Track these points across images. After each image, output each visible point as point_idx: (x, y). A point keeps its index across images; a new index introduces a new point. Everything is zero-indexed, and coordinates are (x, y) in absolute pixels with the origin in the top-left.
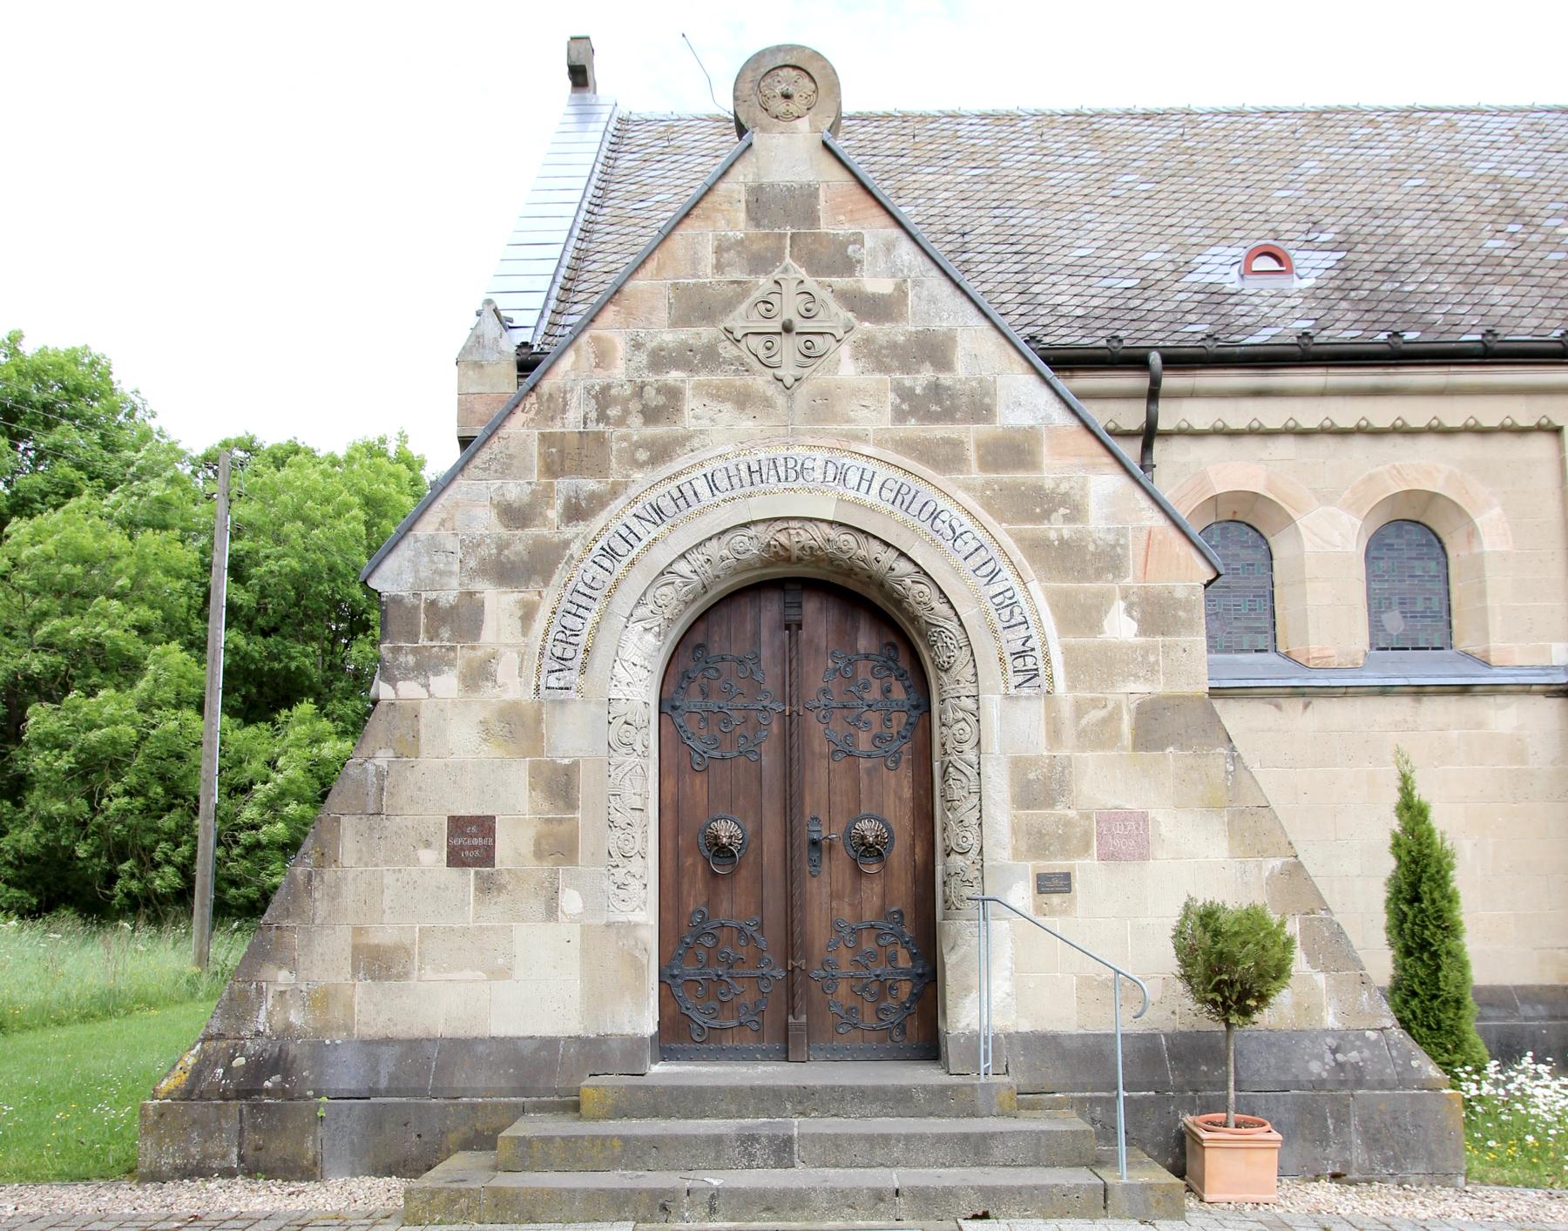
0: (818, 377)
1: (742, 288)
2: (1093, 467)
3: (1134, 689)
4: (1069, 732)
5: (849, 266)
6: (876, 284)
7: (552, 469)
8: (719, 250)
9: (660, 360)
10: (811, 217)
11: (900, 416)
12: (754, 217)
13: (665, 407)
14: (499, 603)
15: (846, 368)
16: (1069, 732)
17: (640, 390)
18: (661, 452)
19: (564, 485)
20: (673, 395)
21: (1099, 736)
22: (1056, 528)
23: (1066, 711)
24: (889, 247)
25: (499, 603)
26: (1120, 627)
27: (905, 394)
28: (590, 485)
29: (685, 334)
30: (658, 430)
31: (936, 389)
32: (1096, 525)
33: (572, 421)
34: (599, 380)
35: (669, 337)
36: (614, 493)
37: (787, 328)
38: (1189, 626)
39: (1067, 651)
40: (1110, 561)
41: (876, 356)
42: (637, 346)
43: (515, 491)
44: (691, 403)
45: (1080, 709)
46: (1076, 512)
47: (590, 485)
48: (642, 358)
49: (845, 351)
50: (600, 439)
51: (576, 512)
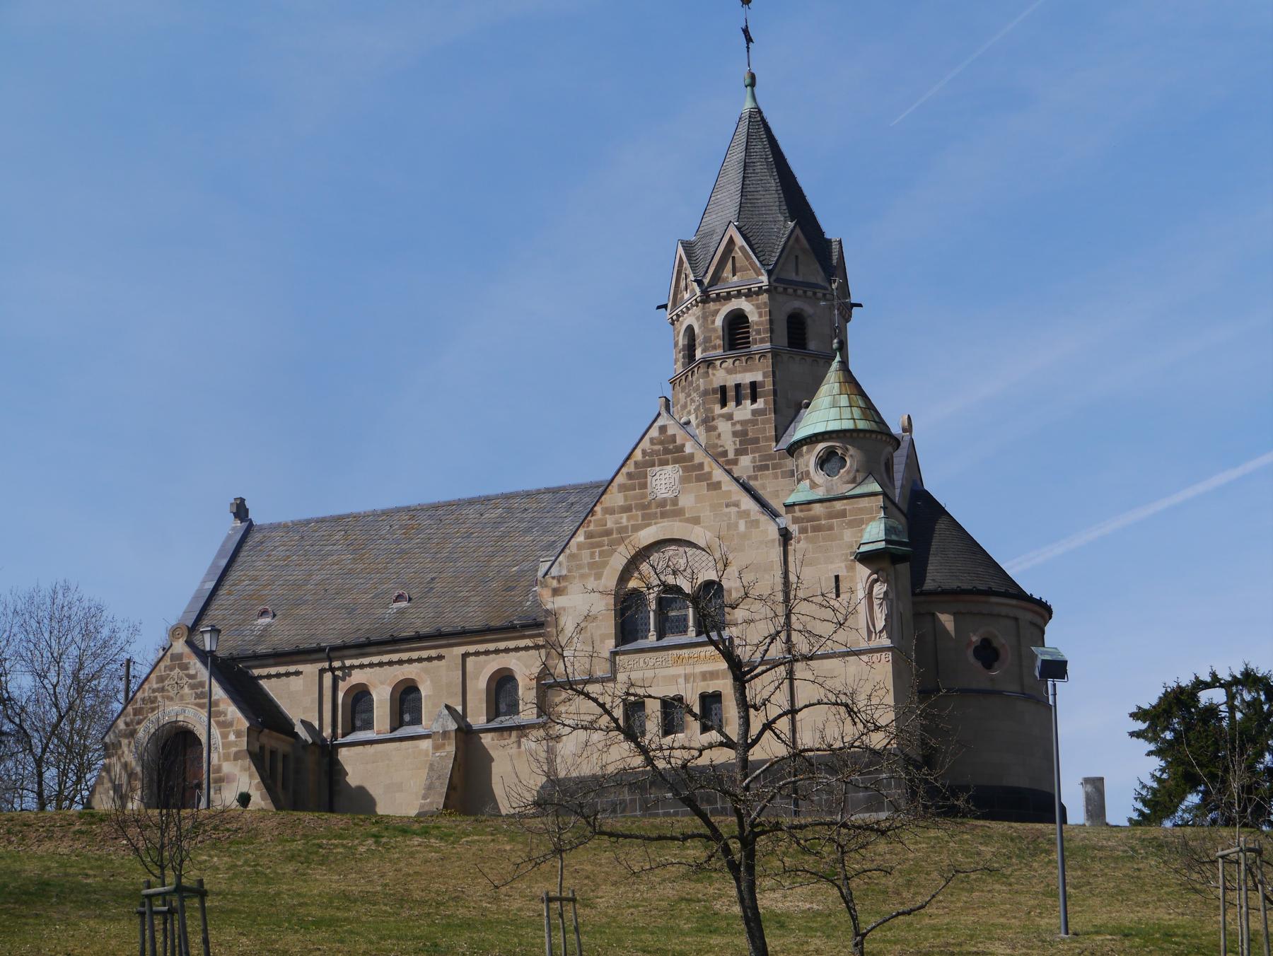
0: (181, 692)
1: (169, 675)
2: (229, 705)
3: (234, 749)
4: (222, 759)
5: (187, 669)
6: (192, 672)
7: (135, 714)
8: (165, 667)
9: (154, 691)
10: (181, 659)
11: (195, 699)
12: (171, 661)
13: (153, 700)
14: (125, 742)
15: (186, 690)
16: (222, 759)
17: (150, 697)
18: (153, 710)
19: (137, 718)
20: (156, 697)
21: (226, 758)
22: (222, 719)
23: (222, 755)
24: (195, 664)
25: (125, 742)
26: (232, 737)
27: (196, 693)
28: (141, 717)
29: (158, 685)
30: (153, 705)
31: (202, 692)
32: (229, 717)
33: (138, 705)
34: (143, 696)
35: (155, 686)
36: (145, 718)
37: (177, 683)
38: (244, 736)
39: (223, 743)
40: (230, 724)
41: (192, 687)
42: (150, 688)
43: (128, 720)
44: (159, 699)
45: (224, 754)
46: (226, 715)
47: (141, 717)
48: (151, 691)
49: (186, 686)
50: (143, 708)
51: (139, 723)
